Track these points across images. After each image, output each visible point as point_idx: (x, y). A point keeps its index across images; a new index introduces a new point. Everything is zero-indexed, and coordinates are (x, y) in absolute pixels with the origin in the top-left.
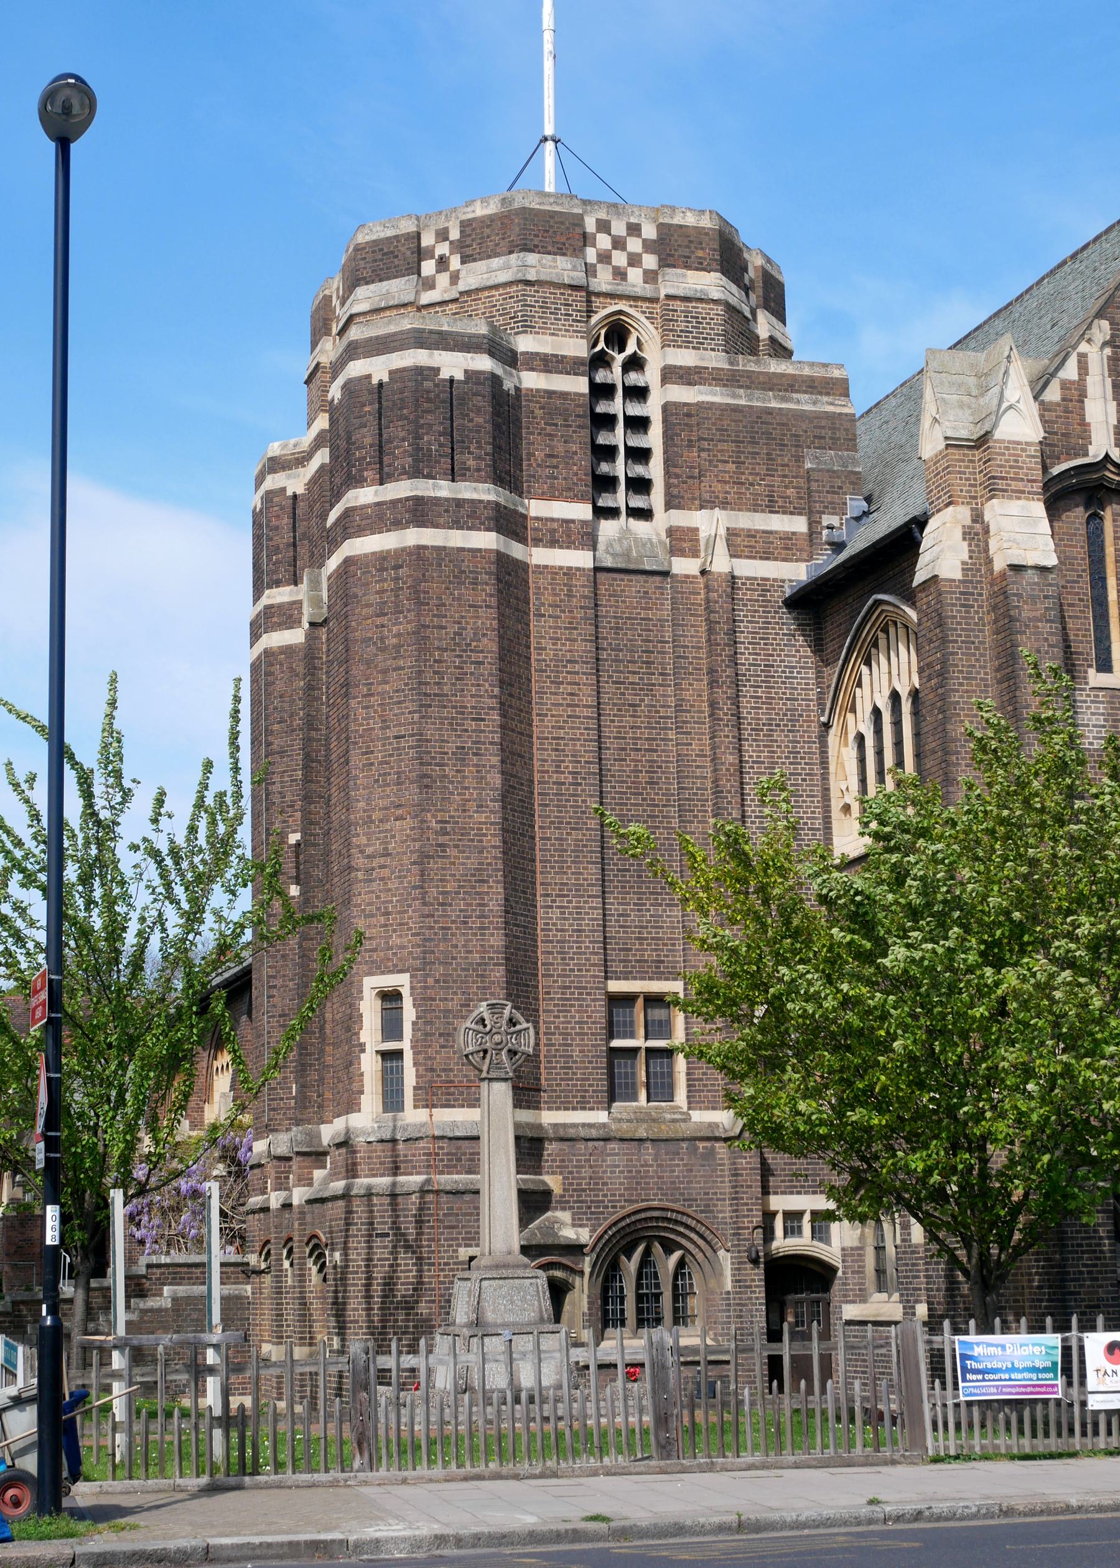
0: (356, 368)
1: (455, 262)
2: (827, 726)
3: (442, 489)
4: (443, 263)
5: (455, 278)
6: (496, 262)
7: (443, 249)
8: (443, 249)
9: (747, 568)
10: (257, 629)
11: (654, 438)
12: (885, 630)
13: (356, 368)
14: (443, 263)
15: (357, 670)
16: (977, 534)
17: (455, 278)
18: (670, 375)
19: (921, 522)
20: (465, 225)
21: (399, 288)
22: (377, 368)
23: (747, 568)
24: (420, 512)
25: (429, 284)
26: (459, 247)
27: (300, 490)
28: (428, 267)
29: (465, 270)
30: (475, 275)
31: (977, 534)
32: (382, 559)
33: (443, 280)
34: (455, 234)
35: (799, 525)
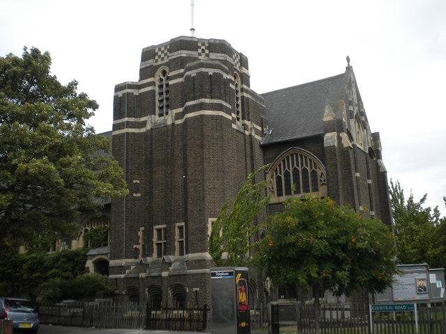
0: (204, 70)
1: (207, 52)
2: (267, 173)
3: (224, 104)
4: (203, 51)
5: (207, 55)
6: (219, 54)
7: (203, 47)
8: (203, 47)
9: (257, 137)
10: (115, 127)
11: (240, 102)
12: (292, 155)
13: (204, 70)
14: (203, 51)
15: (206, 142)
16: (340, 139)
17: (207, 55)
18: (242, 90)
19: (324, 134)
20: (210, 43)
21: (194, 54)
22: (211, 72)
23: (257, 137)
24: (220, 108)
25: (200, 55)
26: (207, 48)
27: (137, 94)
28: (200, 51)
29: (211, 54)
30: (213, 56)
31: (340, 139)
32: (212, 117)
33: (203, 55)
34: (207, 45)
35: (260, 128)
